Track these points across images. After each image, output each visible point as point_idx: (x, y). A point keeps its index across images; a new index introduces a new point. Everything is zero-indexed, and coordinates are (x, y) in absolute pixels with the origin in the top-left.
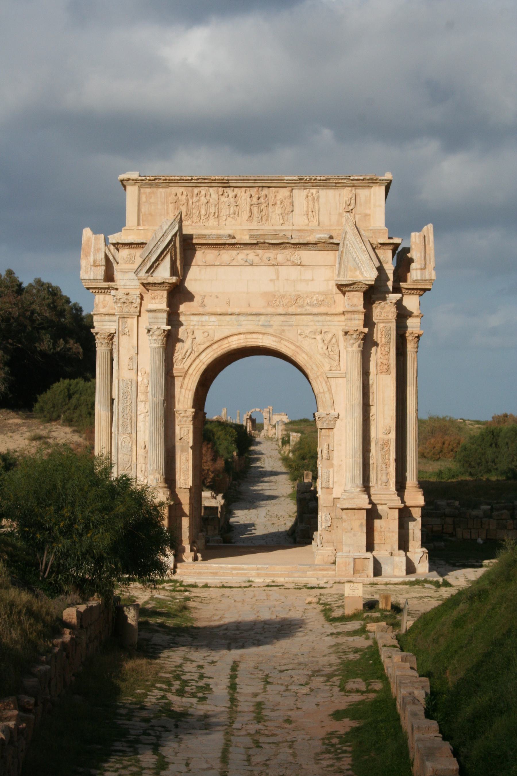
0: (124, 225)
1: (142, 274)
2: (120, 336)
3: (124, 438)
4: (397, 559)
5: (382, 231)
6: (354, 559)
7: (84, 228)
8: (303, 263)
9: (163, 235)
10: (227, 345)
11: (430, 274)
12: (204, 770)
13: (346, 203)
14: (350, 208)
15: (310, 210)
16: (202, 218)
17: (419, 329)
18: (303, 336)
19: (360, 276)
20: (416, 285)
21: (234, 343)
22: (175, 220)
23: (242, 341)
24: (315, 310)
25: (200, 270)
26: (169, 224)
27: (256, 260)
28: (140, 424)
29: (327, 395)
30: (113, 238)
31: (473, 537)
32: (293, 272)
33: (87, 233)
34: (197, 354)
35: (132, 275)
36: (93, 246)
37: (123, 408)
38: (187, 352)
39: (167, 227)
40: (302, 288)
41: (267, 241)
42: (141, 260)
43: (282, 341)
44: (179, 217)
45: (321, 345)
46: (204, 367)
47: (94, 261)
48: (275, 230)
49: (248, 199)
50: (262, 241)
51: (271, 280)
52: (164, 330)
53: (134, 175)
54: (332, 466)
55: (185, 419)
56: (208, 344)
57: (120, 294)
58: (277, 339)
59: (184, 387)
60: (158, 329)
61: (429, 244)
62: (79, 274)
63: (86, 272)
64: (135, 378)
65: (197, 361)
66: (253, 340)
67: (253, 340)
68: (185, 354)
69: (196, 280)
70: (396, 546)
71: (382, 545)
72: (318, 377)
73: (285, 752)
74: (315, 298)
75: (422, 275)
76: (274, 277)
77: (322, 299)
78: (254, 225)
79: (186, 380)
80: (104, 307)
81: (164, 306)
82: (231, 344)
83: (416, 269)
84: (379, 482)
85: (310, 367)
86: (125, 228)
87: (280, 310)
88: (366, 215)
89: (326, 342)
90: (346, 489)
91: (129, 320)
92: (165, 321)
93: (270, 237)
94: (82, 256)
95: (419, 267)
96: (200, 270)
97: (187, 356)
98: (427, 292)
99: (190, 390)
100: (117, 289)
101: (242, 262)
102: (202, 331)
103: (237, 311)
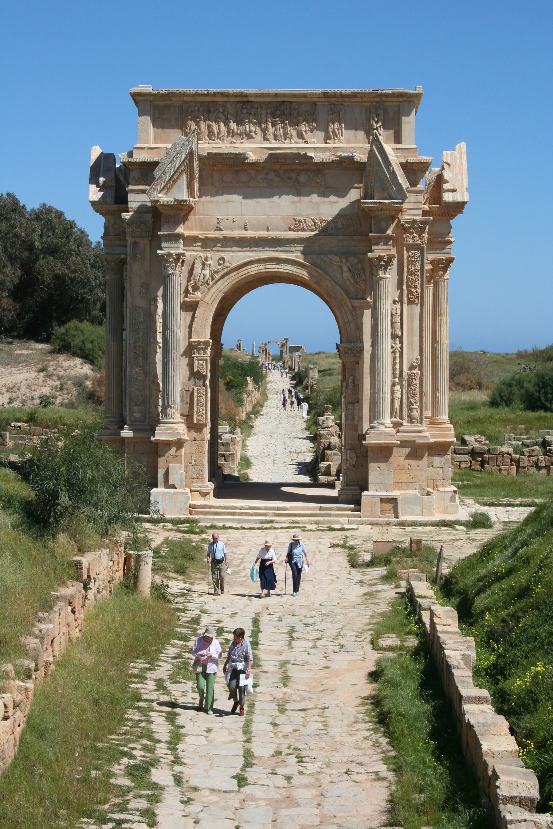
10: (246, 272)
11: (463, 196)
12: (225, 743)
21: (253, 269)
27: (277, 179)
46: (221, 295)
53: (147, 88)
56: (226, 271)
61: (461, 163)
62: (88, 196)
65: (215, 288)
75: (454, 197)
82: (249, 270)
83: (448, 191)
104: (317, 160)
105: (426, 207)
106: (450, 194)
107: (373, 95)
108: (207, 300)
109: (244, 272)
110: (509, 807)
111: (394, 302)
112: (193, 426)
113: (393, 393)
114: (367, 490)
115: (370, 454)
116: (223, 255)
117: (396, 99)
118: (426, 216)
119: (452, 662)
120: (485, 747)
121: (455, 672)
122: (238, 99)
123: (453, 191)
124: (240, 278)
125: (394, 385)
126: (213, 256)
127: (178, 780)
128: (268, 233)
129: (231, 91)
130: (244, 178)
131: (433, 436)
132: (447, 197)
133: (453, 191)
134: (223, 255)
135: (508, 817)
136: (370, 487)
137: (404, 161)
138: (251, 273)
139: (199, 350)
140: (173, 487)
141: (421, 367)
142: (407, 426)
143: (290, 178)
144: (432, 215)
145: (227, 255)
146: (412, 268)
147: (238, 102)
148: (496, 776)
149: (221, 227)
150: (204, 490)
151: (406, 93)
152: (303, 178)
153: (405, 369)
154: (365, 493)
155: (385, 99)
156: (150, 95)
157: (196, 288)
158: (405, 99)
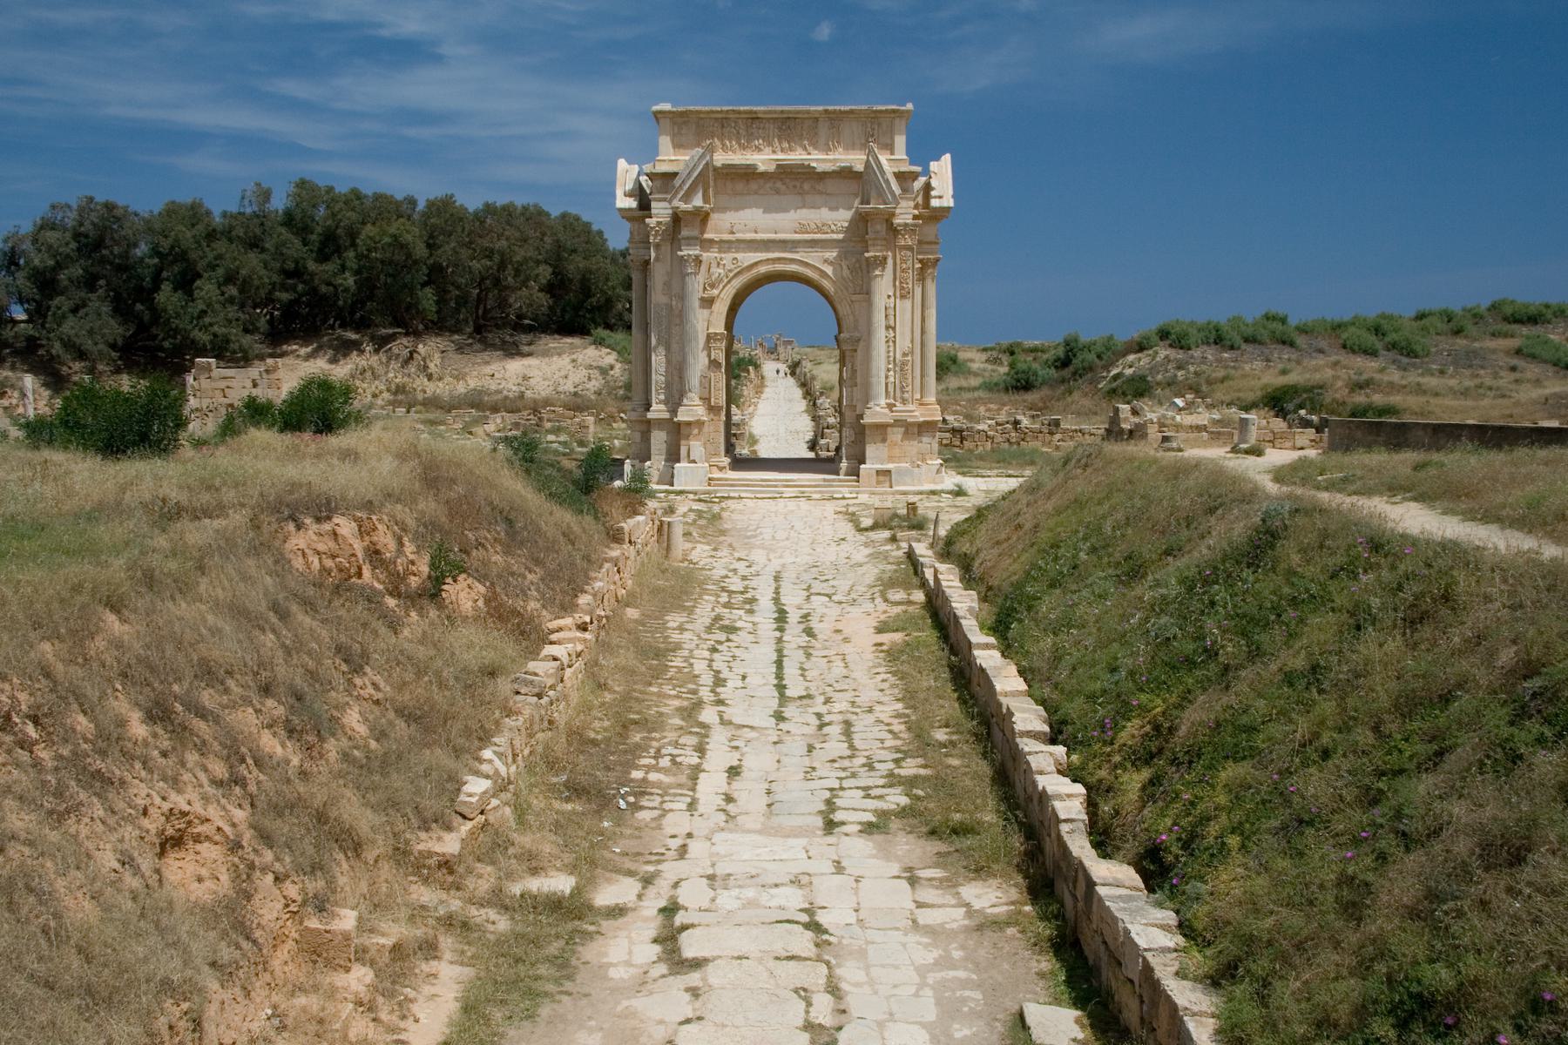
27: (783, 187)
73: (838, 669)
78: (781, 156)
87: (806, 237)
104: (819, 170)
105: (916, 212)
109: (754, 271)
110: (1025, 740)
111: (889, 297)
112: (712, 409)
113: (887, 377)
115: (867, 432)
116: (736, 255)
119: (959, 613)
120: (998, 687)
121: (963, 622)
123: (940, 197)
125: (888, 370)
126: (727, 258)
127: (723, 722)
130: (754, 186)
131: (922, 415)
132: (935, 203)
133: (940, 197)
135: (1027, 749)
139: (715, 340)
140: (694, 462)
141: (912, 353)
142: (900, 407)
143: (795, 187)
145: (739, 256)
146: (904, 266)
148: (1010, 714)
150: (721, 464)
152: (806, 186)
153: (898, 356)
154: (862, 466)
156: (670, 112)
157: (713, 286)
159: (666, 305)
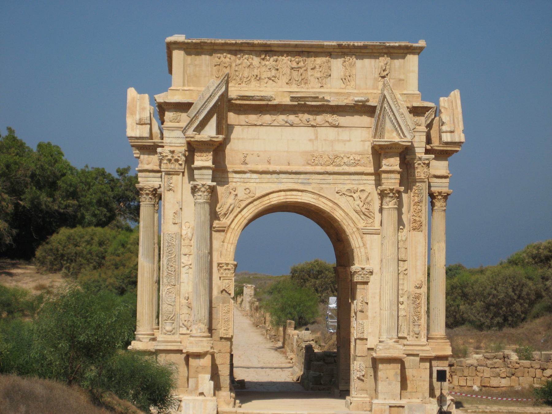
0: (171, 86)
1: (190, 132)
2: (166, 191)
3: (168, 289)
4: (428, 406)
5: (416, 95)
6: (390, 407)
7: (128, 88)
8: (341, 125)
9: (211, 95)
10: (268, 201)
11: (460, 137)
13: (382, 67)
14: (386, 73)
15: (347, 74)
16: (245, 80)
17: (447, 188)
18: (341, 194)
19: (397, 137)
20: (446, 147)
21: (274, 199)
22: (222, 81)
23: (282, 198)
24: (352, 169)
25: (243, 130)
26: (216, 85)
28: (184, 277)
29: (363, 250)
30: (161, 98)
31: (469, 384)
32: (331, 133)
33: (132, 92)
34: (239, 210)
35: (179, 134)
36: (138, 106)
37: (168, 260)
38: (229, 207)
39: (214, 88)
40: (339, 148)
41: (308, 103)
42: (190, 119)
43: (320, 199)
44: (226, 78)
45: (358, 202)
47: (140, 119)
48: (314, 93)
49: (289, 62)
50: (303, 103)
51: (310, 140)
52: (210, 186)
53: (180, 38)
54: (367, 317)
55: (227, 271)
57: (165, 151)
58: (315, 197)
59: (227, 241)
60: (203, 185)
61: (457, 108)
62: (125, 132)
63: (133, 130)
64: (179, 231)
65: (240, 216)
66: (293, 197)
67: (293, 197)
68: (228, 210)
69: (238, 139)
70: (427, 394)
71: (414, 393)
72: (354, 232)
74: (352, 158)
75: (451, 138)
76: (313, 137)
77: (359, 158)
78: (294, 88)
79: (229, 234)
80: (148, 164)
81: (210, 164)
82: (271, 200)
83: (446, 132)
84: (411, 334)
85: (346, 224)
86: (172, 88)
87: (319, 169)
88: (400, 80)
89: (362, 199)
90: (381, 340)
91: (175, 177)
92: (211, 177)
93: (310, 99)
94: (127, 115)
95: (449, 129)
96: (243, 130)
97: (229, 212)
98: (455, 153)
99: (232, 243)
100: (163, 147)
101: (283, 123)
102: (245, 188)
103: (278, 168)
106: (449, 134)
107: (382, 47)
108: (233, 226)
114: (377, 398)
116: (247, 185)
117: (402, 51)
118: (430, 154)
122: (262, 49)
123: (452, 132)
124: (263, 207)
128: (288, 167)
129: (256, 42)
130: (267, 118)
134: (247, 185)
136: (380, 395)
137: (409, 105)
138: (273, 203)
144: (432, 154)
147: (262, 51)
149: (246, 161)
151: (411, 46)
154: (375, 401)
155: (392, 51)
156: (183, 43)
158: (410, 51)
159: (176, 234)
